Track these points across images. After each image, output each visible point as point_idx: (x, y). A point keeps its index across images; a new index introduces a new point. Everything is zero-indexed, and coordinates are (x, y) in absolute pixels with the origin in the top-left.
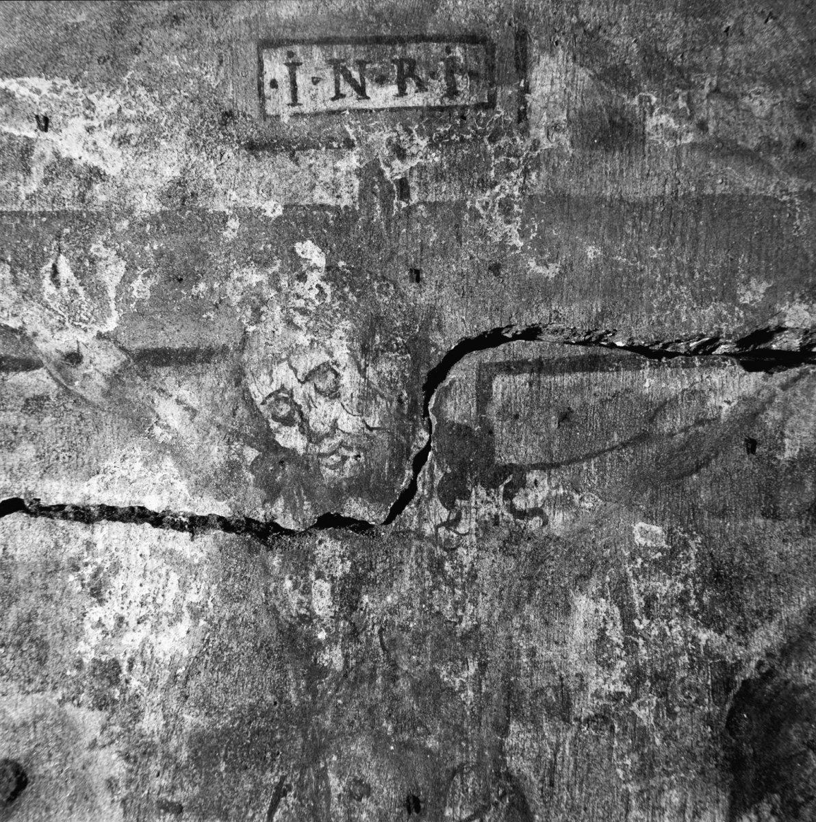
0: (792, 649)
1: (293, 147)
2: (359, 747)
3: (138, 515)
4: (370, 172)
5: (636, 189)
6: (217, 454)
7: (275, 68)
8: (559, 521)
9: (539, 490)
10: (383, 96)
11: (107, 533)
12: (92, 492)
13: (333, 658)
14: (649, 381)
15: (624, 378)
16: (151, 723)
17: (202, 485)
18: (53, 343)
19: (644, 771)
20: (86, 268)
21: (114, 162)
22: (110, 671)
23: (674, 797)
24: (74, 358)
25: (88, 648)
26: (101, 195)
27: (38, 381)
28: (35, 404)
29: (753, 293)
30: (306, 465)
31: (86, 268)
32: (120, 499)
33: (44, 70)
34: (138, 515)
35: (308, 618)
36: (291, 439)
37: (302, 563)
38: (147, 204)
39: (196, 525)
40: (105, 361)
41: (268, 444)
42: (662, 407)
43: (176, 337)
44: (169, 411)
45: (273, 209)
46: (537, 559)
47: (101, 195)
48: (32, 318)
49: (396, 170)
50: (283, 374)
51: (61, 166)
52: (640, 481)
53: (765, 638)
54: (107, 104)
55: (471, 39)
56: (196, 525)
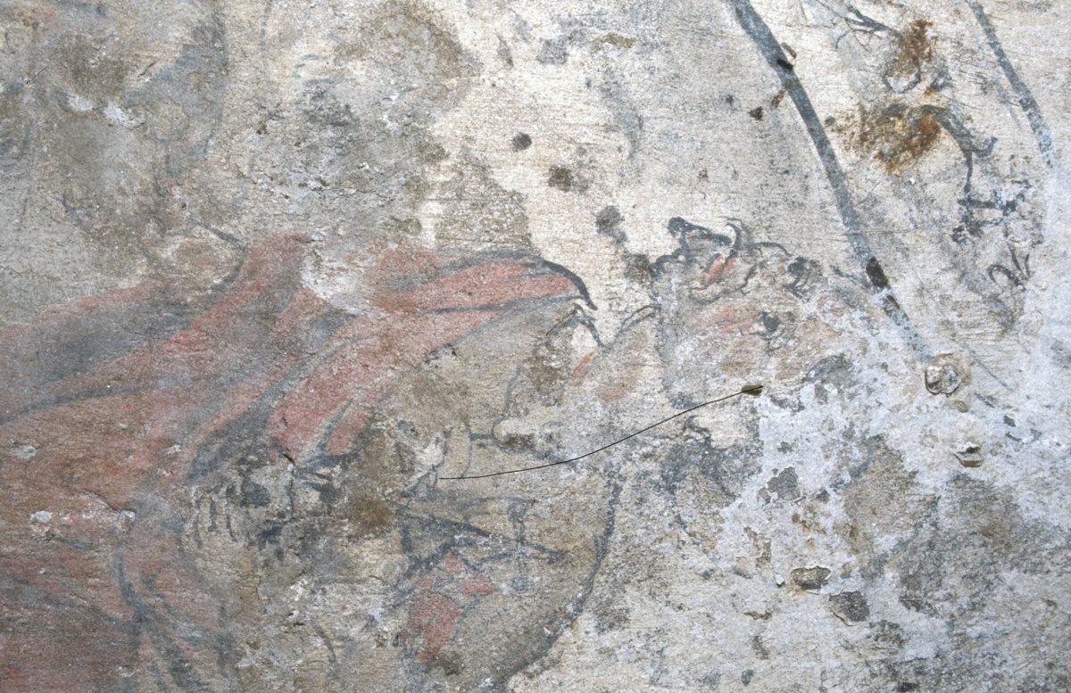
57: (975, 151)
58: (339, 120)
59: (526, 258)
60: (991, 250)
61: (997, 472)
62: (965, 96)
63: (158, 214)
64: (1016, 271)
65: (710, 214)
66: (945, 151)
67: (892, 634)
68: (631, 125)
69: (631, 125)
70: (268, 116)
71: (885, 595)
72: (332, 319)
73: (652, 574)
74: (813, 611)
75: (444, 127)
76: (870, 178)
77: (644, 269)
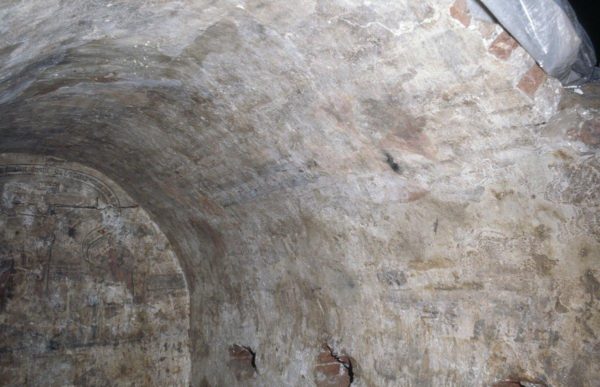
0: (75, 226)
1: (41, 190)
2: (43, 232)
3: (28, 215)
4: (47, 192)
5: (66, 195)
6: (35, 211)
7: (41, 184)
8: (59, 217)
9: (58, 215)
10: (48, 187)
11: (25, 216)
12: (25, 213)
13: (42, 225)
14: (66, 208)
15: (64, 208)
16: (28, 229)
17: (33, 213)
18: (22, 202)
19: (64, 233)
20: (25, 197)
21: (28, 189)
22: (25, 225)
23: (65, 236)
24: (24, 204)
25: (23, 224)
26: (26, 192)
27: (21, 205)
28: (21, 207)
29: (74, 203)
30: (41, 213)
31: (25, 197)
32: (27, 214)
33: (23, 182)
34: (28, 215)
35: (40, 223)
36: (40, 210)
37: (40, 219)
38: (30, 193)
39: (33, 216)
40: (27, 204)
41: (38, 211)
42: (67, 210)
43: (32, 203)
44: (31, 208)
45: (40, 194)
46: (57, 219)
47: (26, 192)
48: (21, 200)
49: (49, 192)
50: (40, 206)
51: (24, 190)
52: (65, 215)
53: (73, 226)
54: (27, 185)
55: (56, 183)
56: (33, 216)
57: (104, 228)
58: (102, 260)
59: (109, 251)
60: (109, 228)
61: (121, 227)
62: (101, 229)
63: (106, 270)
64: (110, 226)
65: (107, 242)
66: (104, 230)
67: (128, 233)
68: (103, 246)
69: (103, 246)
70: (101, 264)
71: (127, 233)
72: (112, 261)
73: (125, 245)
74: (127, 237)
75: (103, 255)
76: (106, 234)
77: (110, 245)
